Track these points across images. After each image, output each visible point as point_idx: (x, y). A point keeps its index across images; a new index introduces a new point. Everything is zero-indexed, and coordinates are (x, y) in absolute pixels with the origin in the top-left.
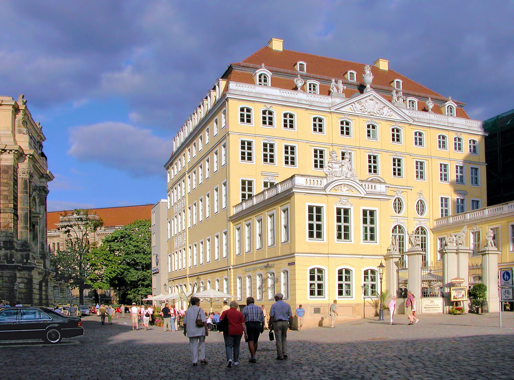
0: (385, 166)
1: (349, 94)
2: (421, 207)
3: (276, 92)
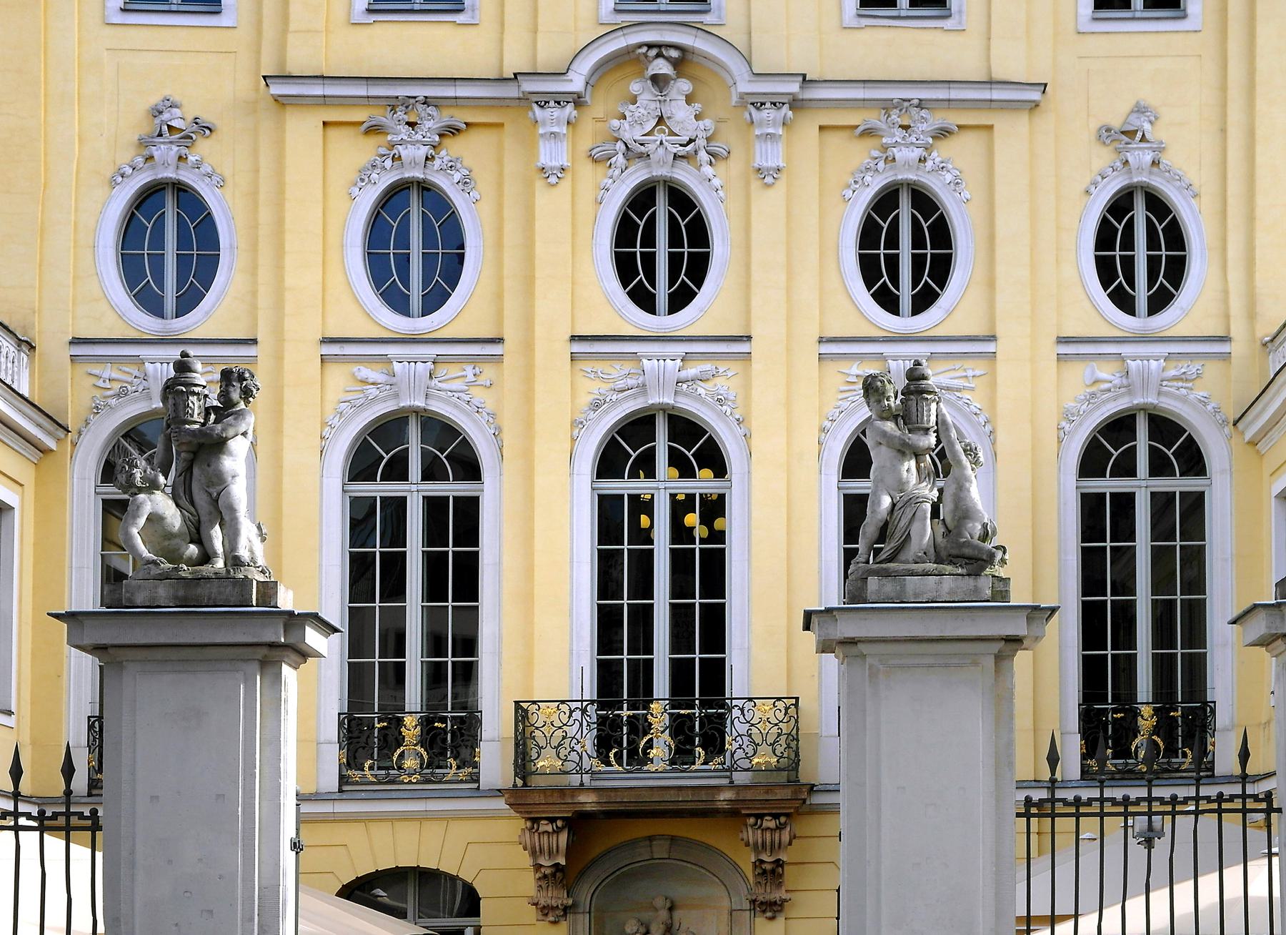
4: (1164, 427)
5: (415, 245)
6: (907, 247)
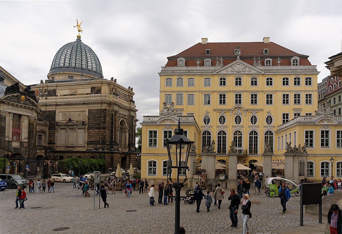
0: (246, 99)
1: (225, 64)
2: (269, 120)
3: (185, 68)
4: (270, 132)
5: (222, 120)
6: (254, 120)
